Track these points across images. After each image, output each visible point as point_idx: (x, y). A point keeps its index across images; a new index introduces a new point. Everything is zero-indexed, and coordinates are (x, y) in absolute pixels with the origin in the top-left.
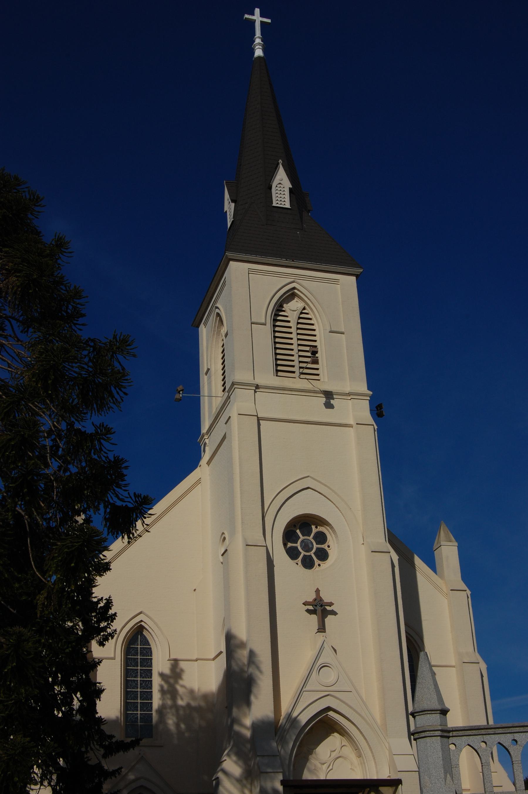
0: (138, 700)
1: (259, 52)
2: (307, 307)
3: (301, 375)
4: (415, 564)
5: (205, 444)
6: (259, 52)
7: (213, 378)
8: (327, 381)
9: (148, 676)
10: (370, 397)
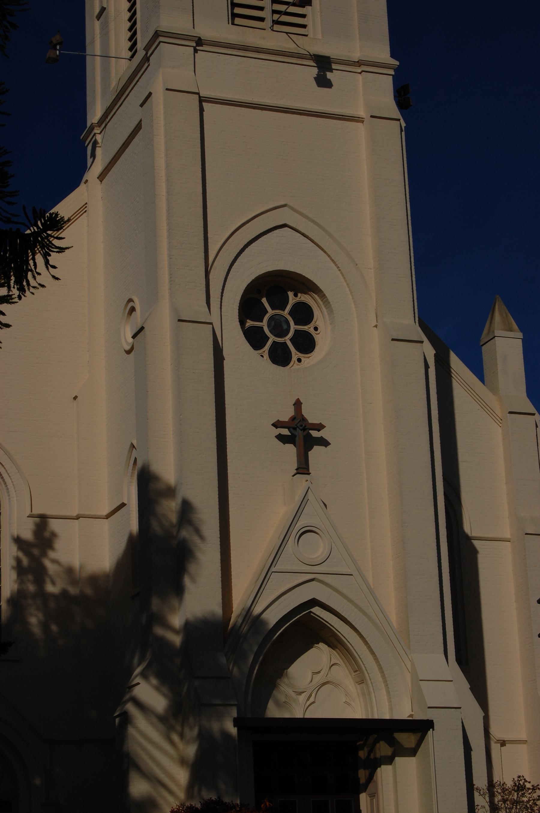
3: (275, 25)
4: (450, 367)
5: (95, 143)
7: (112, 26)
8: (320, 38)
10: (395, 70)
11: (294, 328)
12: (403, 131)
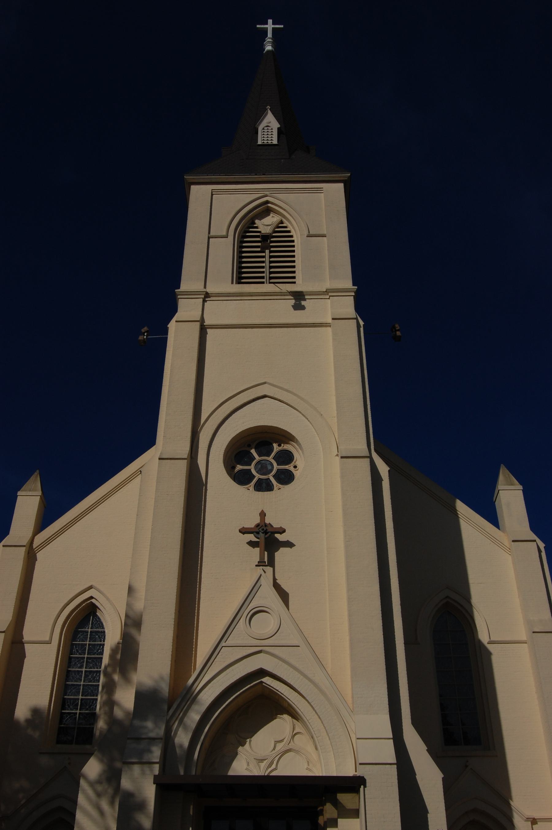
0: (79, 696)
1: (269, 48)
2: (284, 220)
6: (269, 48)
8: (301, 283)
9: (96, 665)
11: (277, 468)
12: (361, 327)
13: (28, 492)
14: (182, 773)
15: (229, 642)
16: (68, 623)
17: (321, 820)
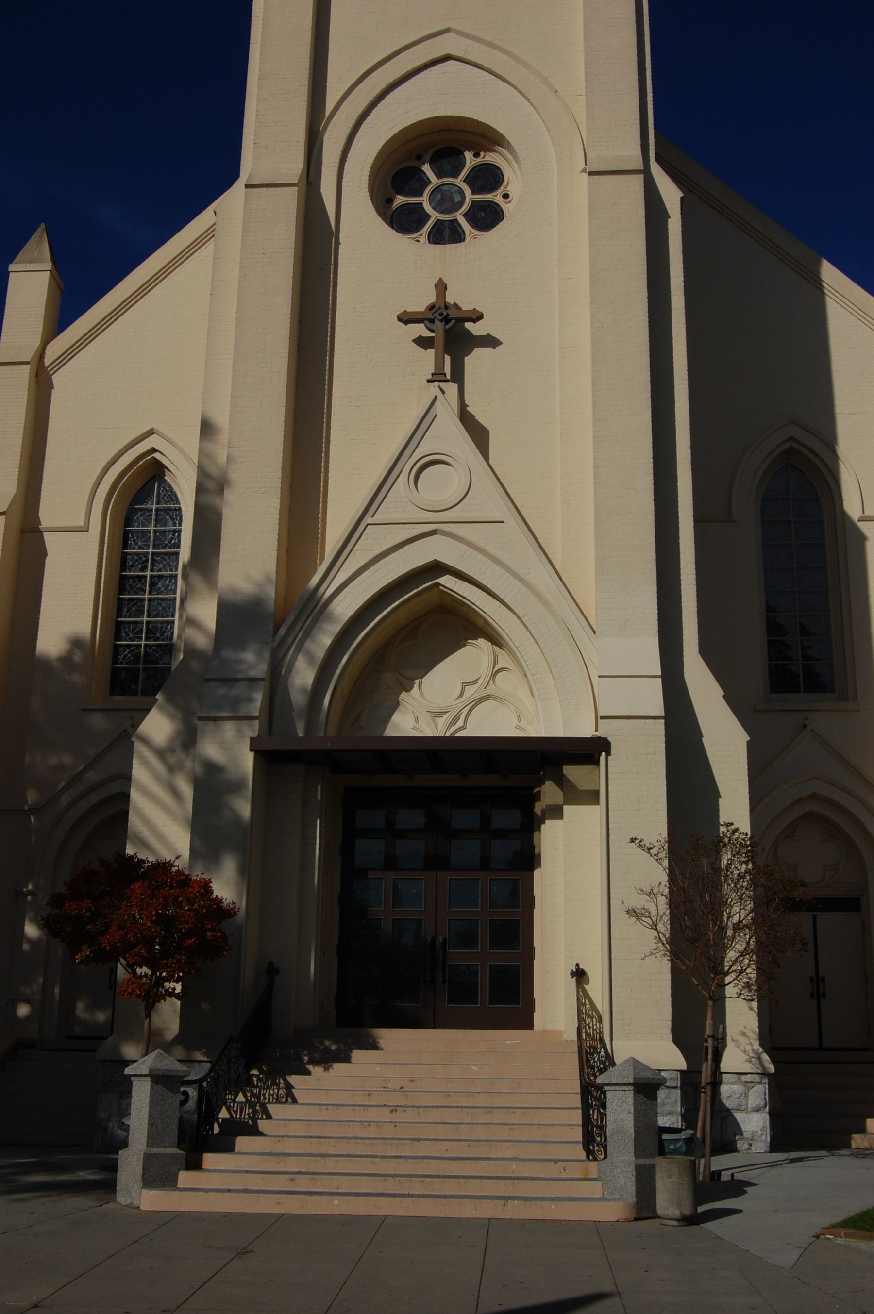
0: (143, 617)
4: (821, 280)
13: (28, 264)
14: (301, 734)
15: (378, 518)
16: (115, 496)
17: (538, 808)
